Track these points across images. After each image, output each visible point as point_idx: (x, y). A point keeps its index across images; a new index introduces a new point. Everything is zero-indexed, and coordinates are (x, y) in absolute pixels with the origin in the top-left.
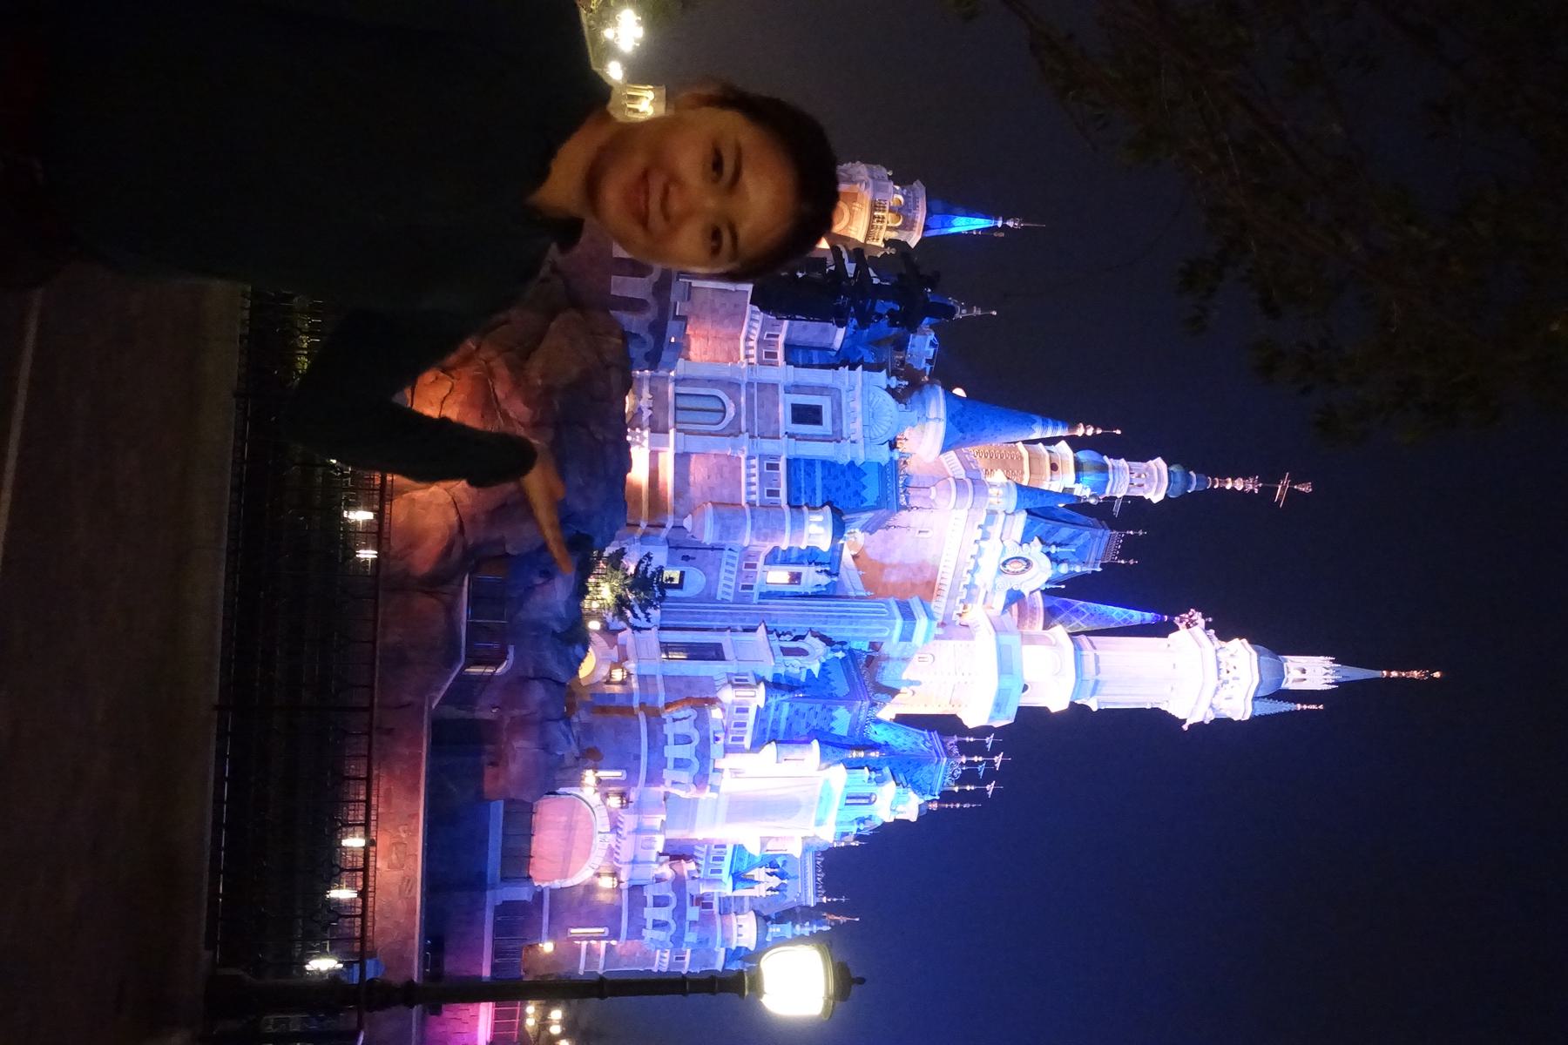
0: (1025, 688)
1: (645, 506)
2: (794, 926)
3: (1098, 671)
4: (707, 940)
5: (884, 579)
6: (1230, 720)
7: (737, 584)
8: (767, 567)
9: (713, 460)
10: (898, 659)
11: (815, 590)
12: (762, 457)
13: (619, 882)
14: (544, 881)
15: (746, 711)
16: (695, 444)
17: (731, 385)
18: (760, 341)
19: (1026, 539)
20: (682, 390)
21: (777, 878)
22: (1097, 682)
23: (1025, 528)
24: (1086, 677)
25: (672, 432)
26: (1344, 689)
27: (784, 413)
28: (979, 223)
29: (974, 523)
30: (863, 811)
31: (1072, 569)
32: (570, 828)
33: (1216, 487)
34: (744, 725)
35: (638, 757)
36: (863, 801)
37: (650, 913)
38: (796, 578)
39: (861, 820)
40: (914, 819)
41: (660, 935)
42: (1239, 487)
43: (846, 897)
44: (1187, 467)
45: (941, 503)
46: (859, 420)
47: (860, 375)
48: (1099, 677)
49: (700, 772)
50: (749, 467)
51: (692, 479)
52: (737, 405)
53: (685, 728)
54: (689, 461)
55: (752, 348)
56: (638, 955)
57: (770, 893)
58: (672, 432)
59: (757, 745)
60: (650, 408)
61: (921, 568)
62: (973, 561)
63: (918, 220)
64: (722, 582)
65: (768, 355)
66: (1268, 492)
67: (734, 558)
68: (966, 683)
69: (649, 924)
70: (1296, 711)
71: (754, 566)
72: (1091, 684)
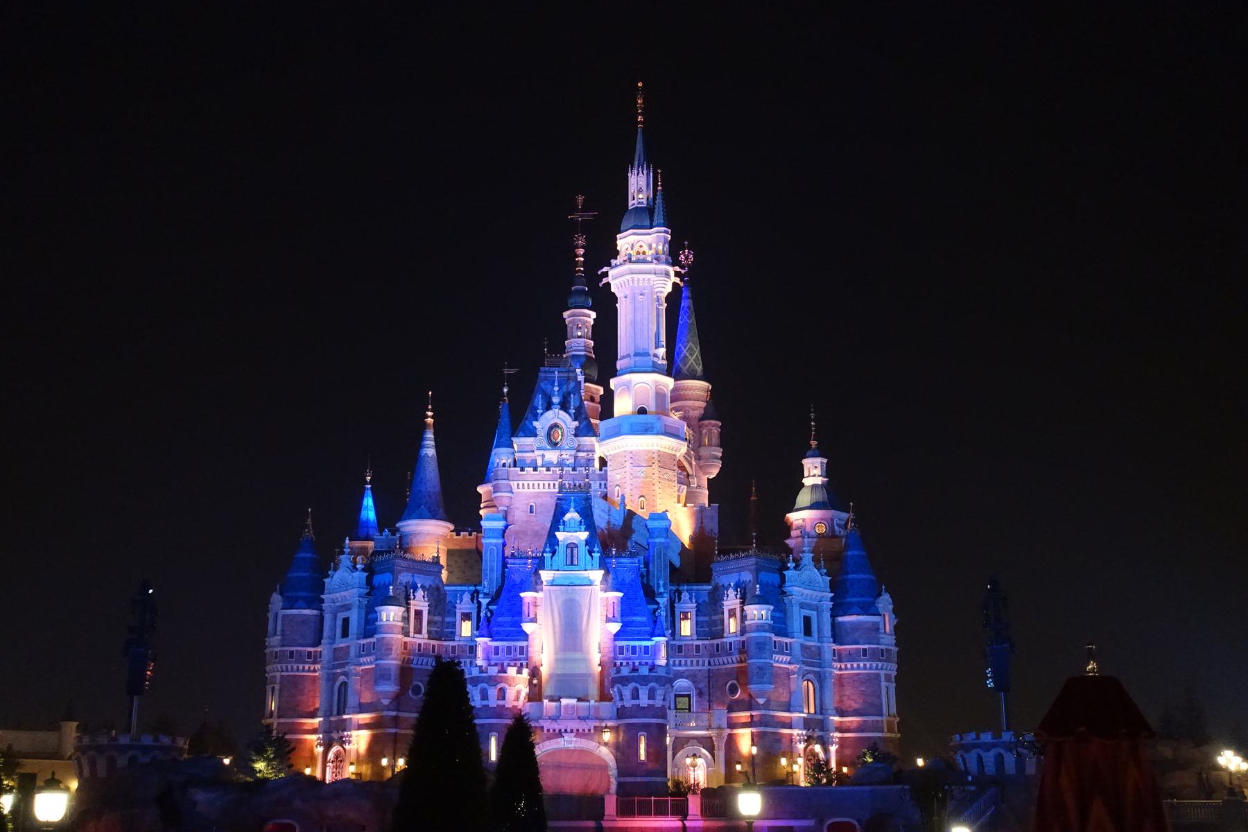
0: (642, 411)
2: (788, 568)
4: (757, 644)
8: (457, 638)
10: (609, 515)
13: (606, 727)
14: (609, 781)
15: (497, 649)
16: (352, 701)
17: (331, 678)
18: (315, 662)
19: (533, 433)
20: (335, 712)
21: (729, 591)
22: (636, 354)
23: (526, 436)
25: (345, 717)
27: (341, 643)
28: (368, 501)
29: (521, 475)
30: (583, 550)
31: (556, 393)
32: (559, 767)
33: (582, 269)
34: (509, 648)
36: (575, 551)
37: (629, 703)
38: (467, 617)
39: (591, 552)
40: (805, 462)
41: (660, 693)
42: (581, 251)
43: (752, 532)
44: (571, 293)
45: (506, 502)
46: (343, 593)
47: (327, 595)
48: (632, 355)
49: (486, 683)
50: (364, 664)
51: (369, 701)
54: (365, 703)
55: (304, 667)
57: (738, 596)
58: (345, 717)
59: (525, 636)
60: (338, 732)
62: (552, 469)
63: (360, 545)
65: (309, 657)
68: (631, 458)
69: (635, 702)
70: (662, 190)
71: (454, 647)
72: (638, 358)
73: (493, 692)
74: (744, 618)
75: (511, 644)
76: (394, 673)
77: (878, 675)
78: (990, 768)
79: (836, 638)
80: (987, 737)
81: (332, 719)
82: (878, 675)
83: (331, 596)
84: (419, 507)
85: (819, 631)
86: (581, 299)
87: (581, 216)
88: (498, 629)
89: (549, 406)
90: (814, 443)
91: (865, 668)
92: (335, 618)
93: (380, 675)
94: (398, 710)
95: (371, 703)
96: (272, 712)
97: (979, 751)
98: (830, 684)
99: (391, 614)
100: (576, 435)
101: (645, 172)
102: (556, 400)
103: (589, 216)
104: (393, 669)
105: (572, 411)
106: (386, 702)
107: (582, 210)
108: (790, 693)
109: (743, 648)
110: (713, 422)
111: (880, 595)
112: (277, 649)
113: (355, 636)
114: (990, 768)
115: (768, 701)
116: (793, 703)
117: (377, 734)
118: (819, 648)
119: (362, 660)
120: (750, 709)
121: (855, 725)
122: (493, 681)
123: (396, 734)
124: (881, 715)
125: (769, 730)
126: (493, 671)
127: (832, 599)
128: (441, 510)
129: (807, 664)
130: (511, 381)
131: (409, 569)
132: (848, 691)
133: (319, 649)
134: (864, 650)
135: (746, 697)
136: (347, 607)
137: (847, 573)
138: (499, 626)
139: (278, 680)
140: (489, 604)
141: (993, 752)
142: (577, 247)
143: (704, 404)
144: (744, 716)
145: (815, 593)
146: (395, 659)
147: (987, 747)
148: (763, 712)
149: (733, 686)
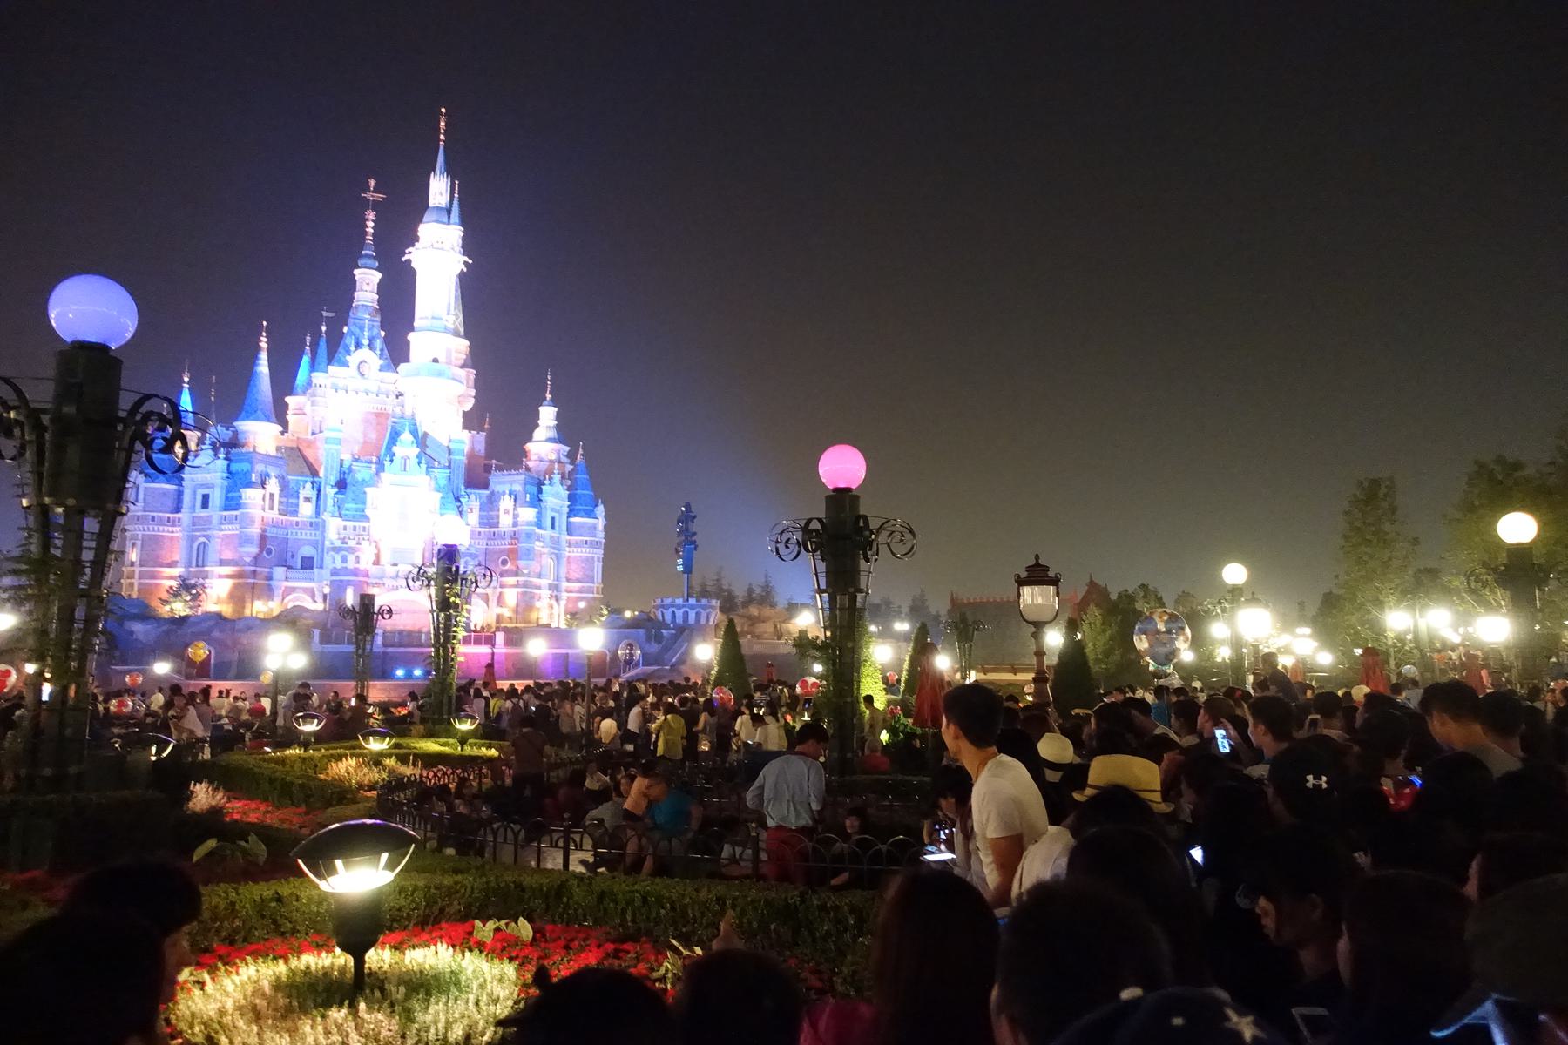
1: (240, 581)
3: (427, 318)
4: (527, 534)
5: (374, 441)
6: (464, 239)
7: (309, 530)
8: (299, 515)
9: (223, 548)
11: (315, 489)
12: (221, 524)
16: (212, 555)
17: (192, 539)
18: (174, 525)
19: (346, 365)
22: (433, 318)
24: (429, 324)
26: (450, 170)
27: (204, 513)
35: (341, 581)
36: (408, 461)
38: (308, 500)
44: (361, 256)
47: (188, 476)
48: (430, 317)
49: (347, 551)
50: (226, 530)
52: (200, 536)
53: (338, 558)
56: (583, 565)
59: (367, 519)
61: (366, 421)
64: (309, 538)
65: (169, 521)
66: (376, 206)
67: (292, 533)
71: (297, 523)
72: (434, 321)
73: (351, 558)
74: (515, 516)
75: (357, 524)
76: (256, 539)
77: (593, 558)
78: (679, 620)
79: (569, 533)
80: (679, 601)
81: (191, 569)
82: (593, 558)
83: (193, 476)
84: (255, 412)
85: (560, 527)
86: (370, 262)
87: (372, 196)
88: (347, 512)
89: (358, 345)
90: (549, 397)
91: (586, 552)
92: (195, 493)
93: (244, 540)
94: (256, 565)
95: (233, 560)
96: (132, 564)
97: (674, 609)
98: (564, 561)
99: (251, 496)
100: (380, 370)
101: (445, 179)
102: (366, 342)
103: (379, 197)
104: (255, 535)
105: (378, 352)
106: (248, 560)
107: (373, 192)
108: (541, 567)
109: (514, 536)
110: (471, 370)
111: (596, 506)
112: (140, 514)
113: (218, 509)
114: (679, 620)
115: (529, 573)
116: (543, 573)
117: (239, 583)
118: (559, 538)
119: (223, 527)
120: (516, 574)
121: (576, 589)
122: (351, 550)
123: (254, 583)
124: (593, 583)
125: (529, 590)
126: (352, 543)
127: (568, 507)
128: (274, 417)
129: (554, 548)
130: (329, 321)
131: (262, 462)
132: (573, 566)
133: (177, 515)
134: (586, 541)
135: (514, 568)
136: (212, 486)
137: (576, 489)
138: (347, 510)
139: (140, 537)
140: (336, 493)
141: (671, 610)
142: (368, 220)
143: (465, 357)
144: (511, 580)
145: (559, 502)
146: (257, 528)
147: (679, 607)
148: (526, 579)
149: (504, 560)
